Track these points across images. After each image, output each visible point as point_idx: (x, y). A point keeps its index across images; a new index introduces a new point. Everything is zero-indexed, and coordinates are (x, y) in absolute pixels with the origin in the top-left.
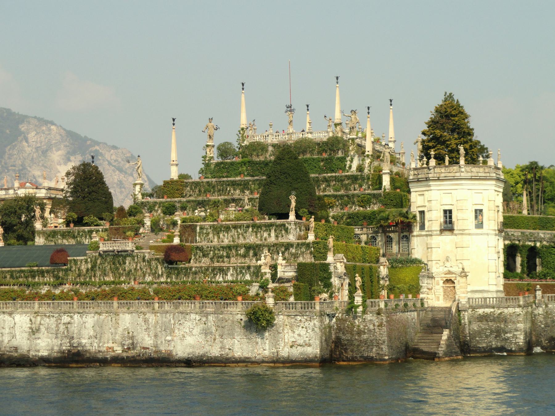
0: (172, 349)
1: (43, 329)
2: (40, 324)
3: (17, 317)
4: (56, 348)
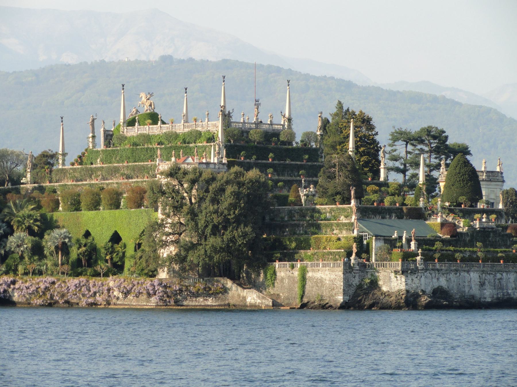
1: (487, 283)
2: (485, 279)
3: (472, 274)
4: (495, 296)
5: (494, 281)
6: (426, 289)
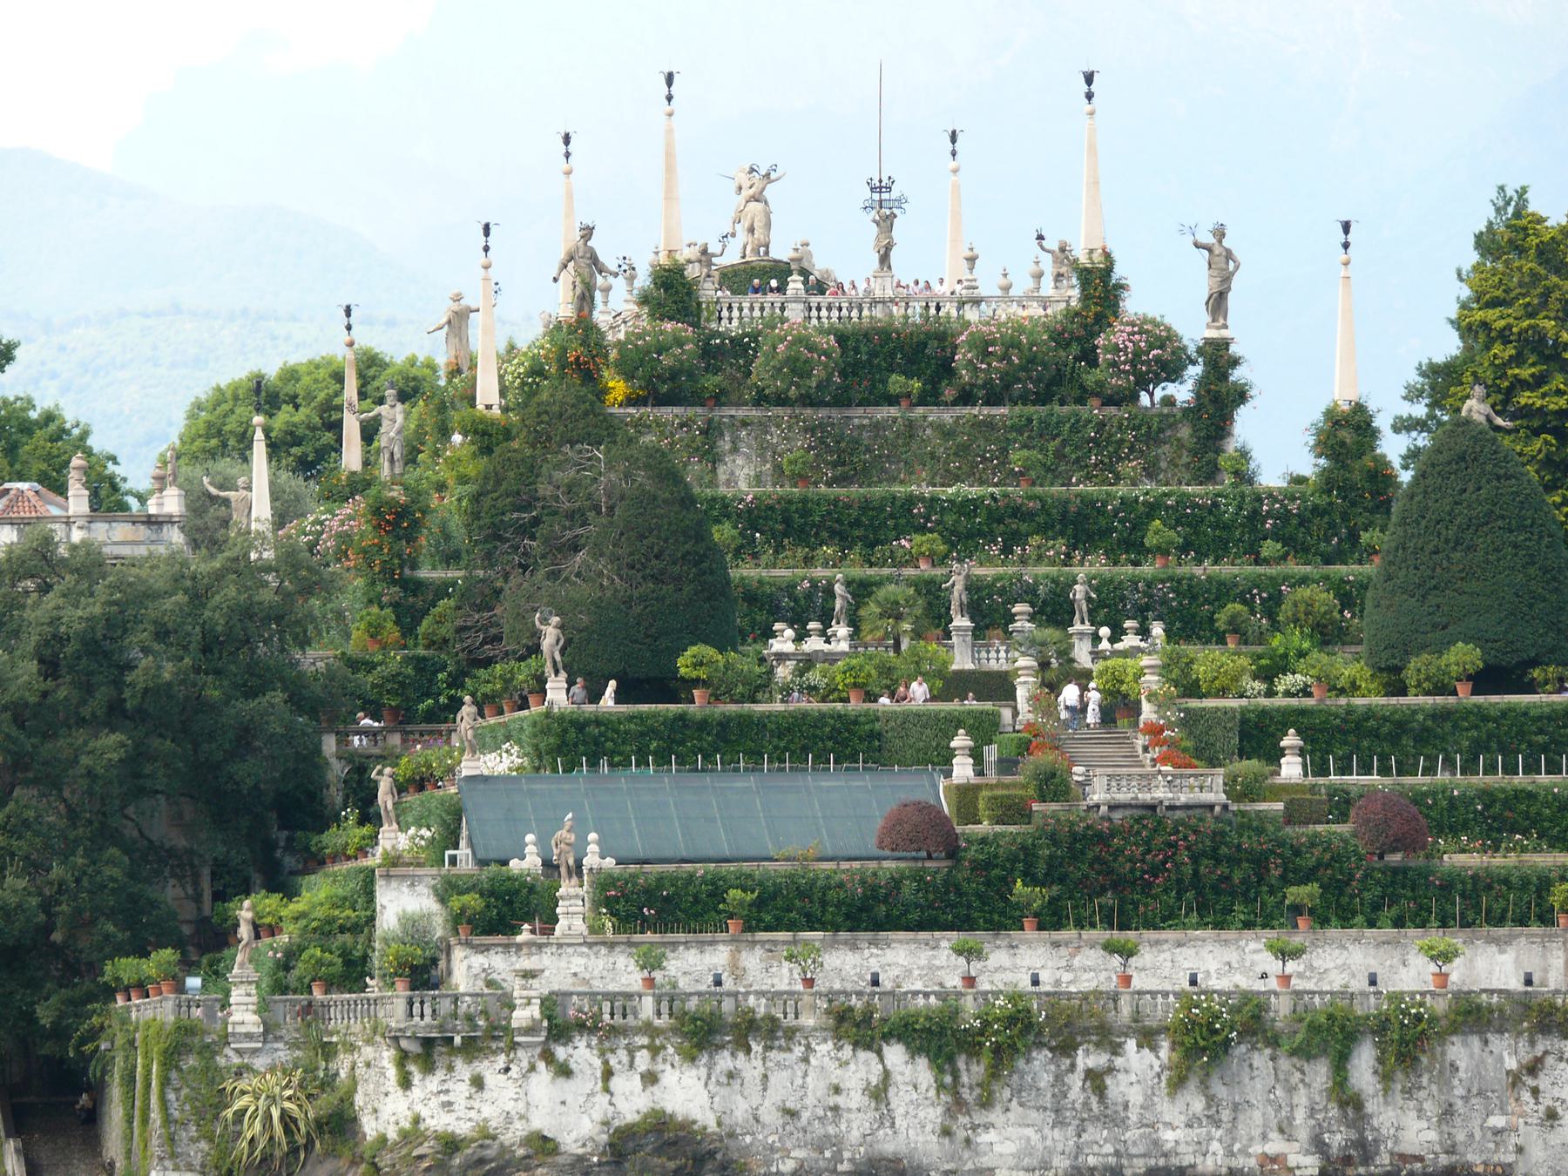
0: (1510, 1158)
5: (1058, 1078)
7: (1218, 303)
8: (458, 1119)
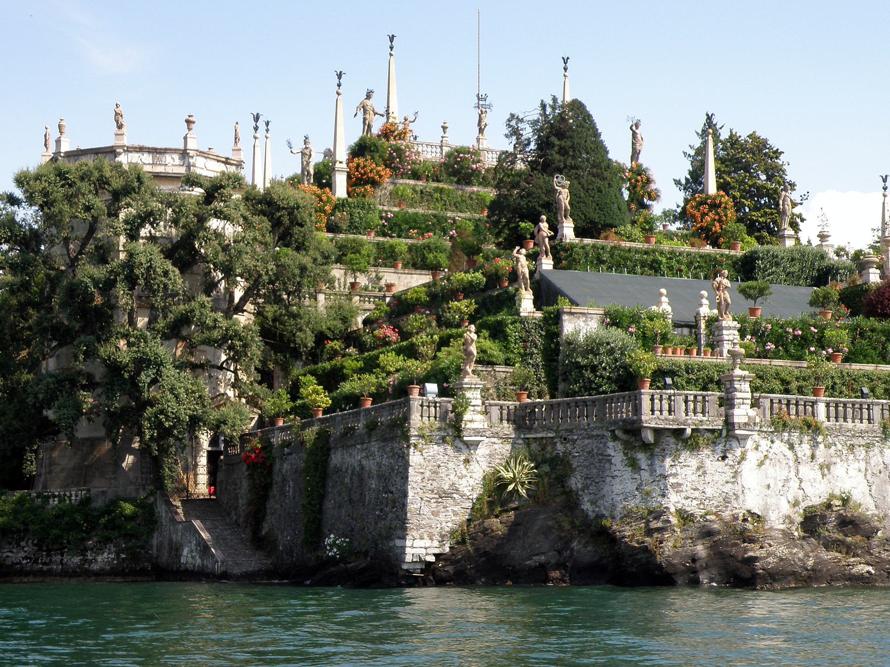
6: (766, 508)
7: (635, 155)
8: (687, 498)
